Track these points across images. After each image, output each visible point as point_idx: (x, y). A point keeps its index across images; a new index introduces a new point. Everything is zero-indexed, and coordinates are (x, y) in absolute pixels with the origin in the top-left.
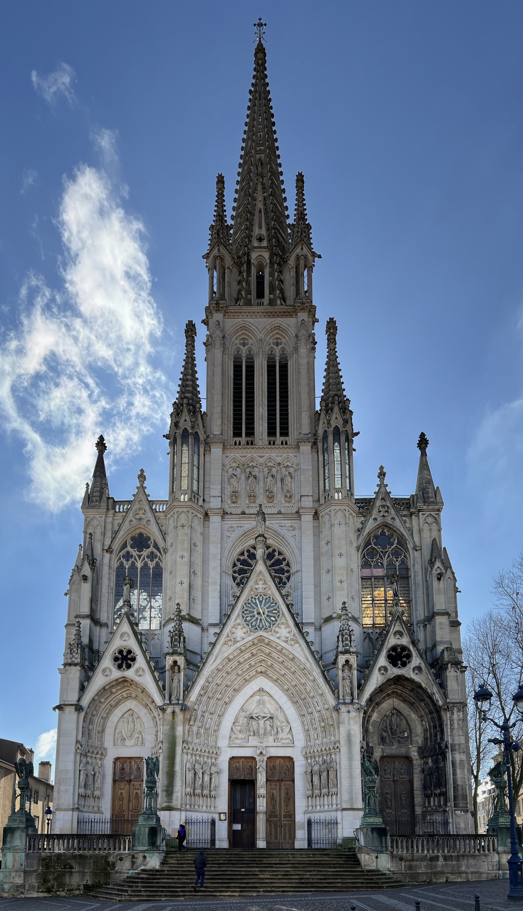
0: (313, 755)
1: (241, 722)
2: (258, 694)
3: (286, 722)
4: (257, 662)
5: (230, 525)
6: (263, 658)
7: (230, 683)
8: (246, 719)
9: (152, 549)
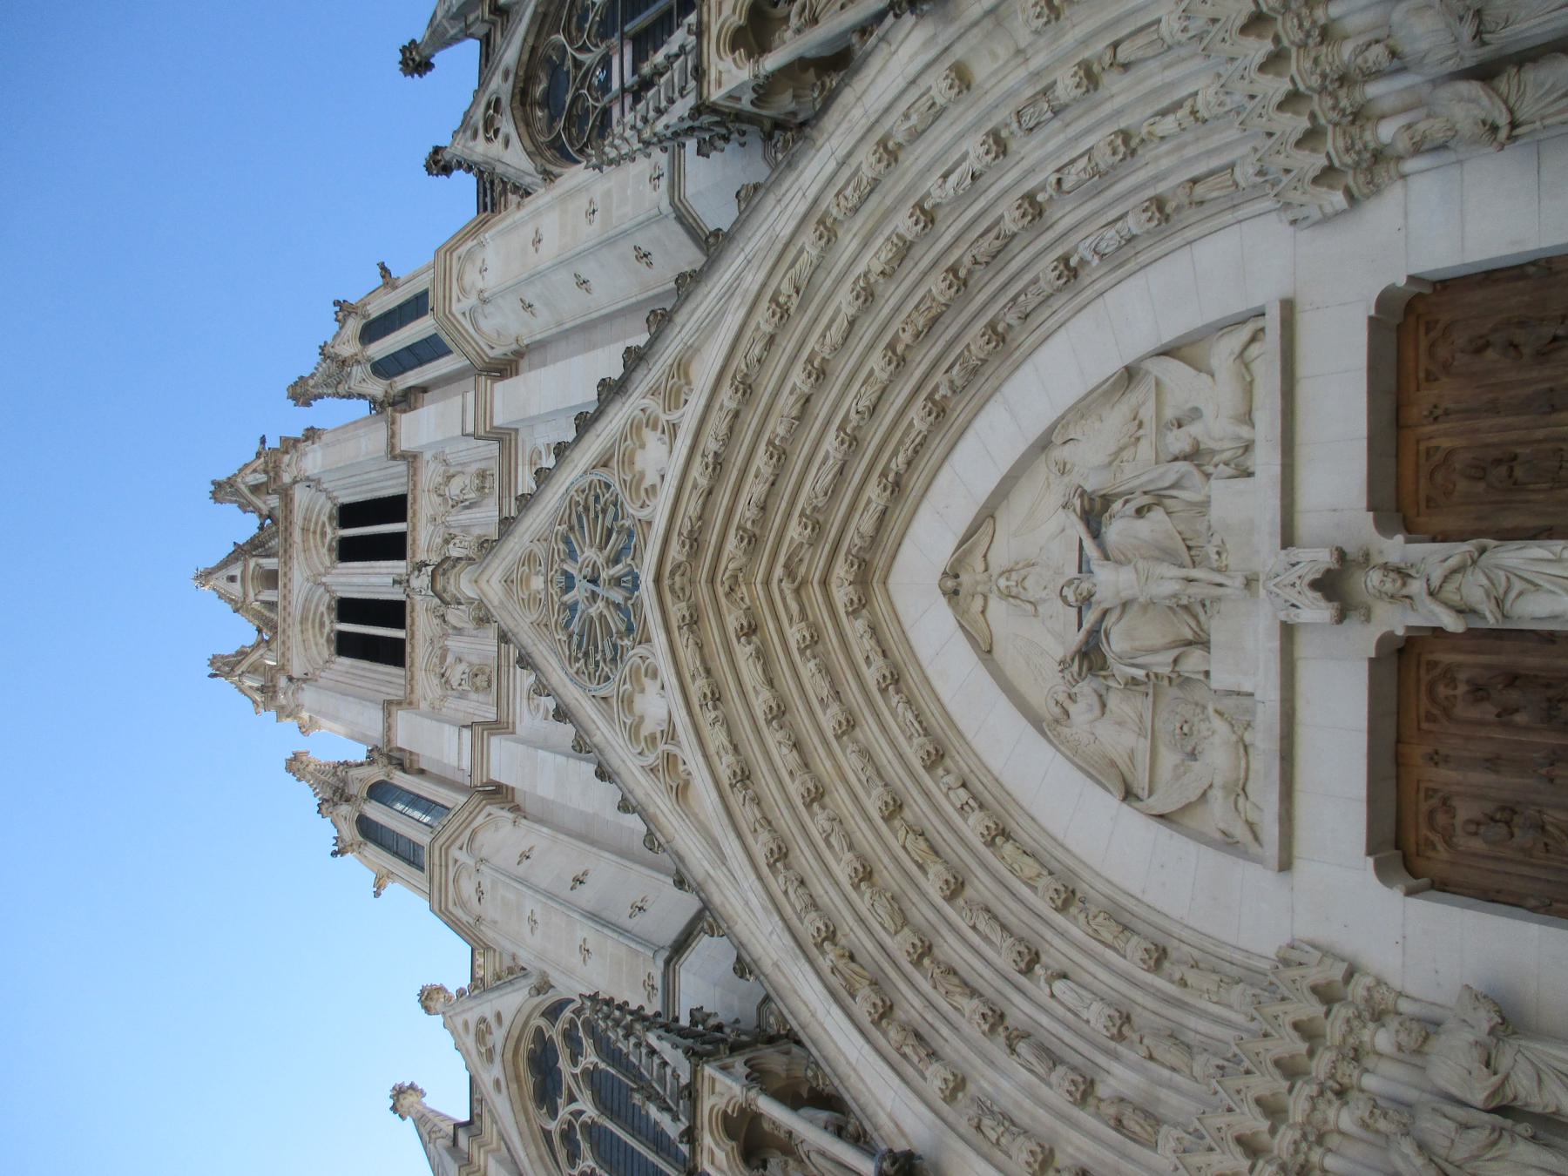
0: (1321, 106)
2: (978, 604)
3: (1133, 398)
4: (794, 607)
5: (525, 701)
6: (779, 571)
8: (1113, 701)
9: (555, 1033)
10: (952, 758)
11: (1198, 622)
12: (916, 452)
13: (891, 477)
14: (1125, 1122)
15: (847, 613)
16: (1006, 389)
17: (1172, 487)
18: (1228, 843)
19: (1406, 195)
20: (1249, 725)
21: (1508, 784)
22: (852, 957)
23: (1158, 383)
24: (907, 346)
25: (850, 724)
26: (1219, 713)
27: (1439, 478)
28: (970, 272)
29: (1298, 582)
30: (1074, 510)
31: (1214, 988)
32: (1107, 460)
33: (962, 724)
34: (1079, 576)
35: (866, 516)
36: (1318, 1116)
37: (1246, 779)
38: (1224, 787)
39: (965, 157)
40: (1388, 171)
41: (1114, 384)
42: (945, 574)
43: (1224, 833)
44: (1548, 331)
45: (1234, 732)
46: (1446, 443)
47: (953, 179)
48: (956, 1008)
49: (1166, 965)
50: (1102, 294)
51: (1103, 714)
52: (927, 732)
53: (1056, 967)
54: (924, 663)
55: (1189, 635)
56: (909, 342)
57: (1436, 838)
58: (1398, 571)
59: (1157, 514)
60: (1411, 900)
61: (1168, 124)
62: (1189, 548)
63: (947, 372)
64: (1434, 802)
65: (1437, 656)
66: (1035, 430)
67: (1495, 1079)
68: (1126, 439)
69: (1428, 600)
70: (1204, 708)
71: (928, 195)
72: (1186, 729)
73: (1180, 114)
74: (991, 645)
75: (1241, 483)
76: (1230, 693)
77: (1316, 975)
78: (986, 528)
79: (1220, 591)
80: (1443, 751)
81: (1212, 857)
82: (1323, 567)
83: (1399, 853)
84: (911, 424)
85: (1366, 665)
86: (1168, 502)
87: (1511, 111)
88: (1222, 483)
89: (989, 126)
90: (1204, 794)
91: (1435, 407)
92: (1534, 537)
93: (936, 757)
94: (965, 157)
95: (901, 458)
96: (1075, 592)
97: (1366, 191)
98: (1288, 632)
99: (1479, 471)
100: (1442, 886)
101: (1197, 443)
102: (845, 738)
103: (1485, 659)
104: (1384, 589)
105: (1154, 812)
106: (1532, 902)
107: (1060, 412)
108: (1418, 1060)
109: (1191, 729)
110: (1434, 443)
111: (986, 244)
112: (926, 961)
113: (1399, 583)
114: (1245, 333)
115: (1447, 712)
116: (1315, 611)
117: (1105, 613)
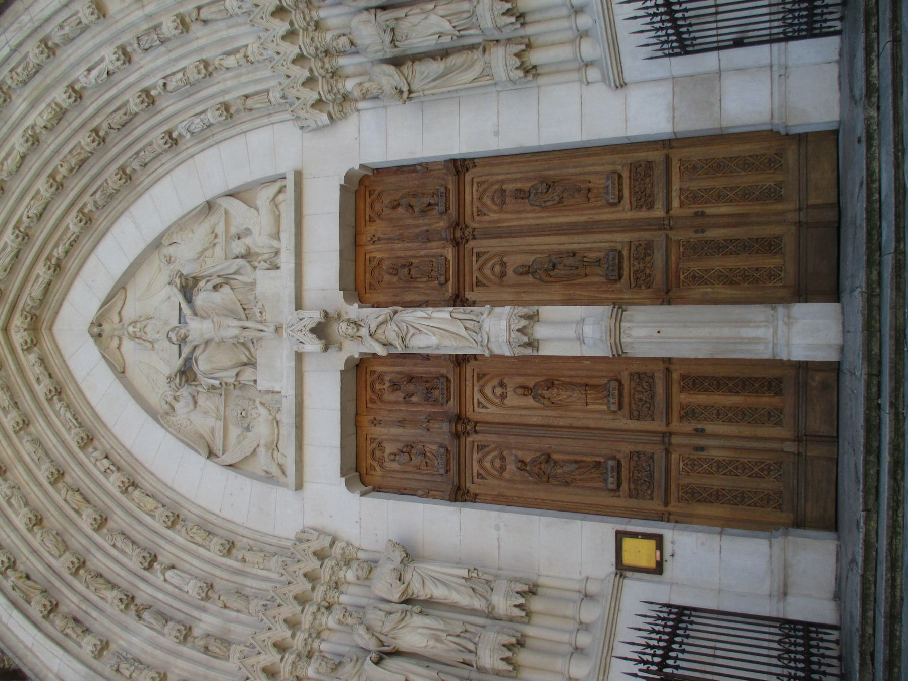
0: (316, 64)
1: (211, 422)
7: (46, 465)
8: (201, 400)
10: (99, 440)
11: (250, 352)
12: (71, 245)
13: (54, 261)
14: (210, 648)
15: (23, 350)
16: (135, 209)
17: (234, 273)
18: (268, 478)
19: (359, 121)
20: (279, 410)
21: (408, 433)
22: (28, 577)
23: (226, 212)
24: (64, 177)
25: (25, 423)
26: (262, 403)
27: (376, 273)
28: (107, 133)
29: (304, 329)
30: (176, 286)
31: (261, 561)
32: (196, 256)
33: (105, 419)
34: (178, 325)
35: (36, 286)
36: (317, 622)
37: (278, 440)
38: (266, 446)
39: (102, 60)
40: (350, 106)
41: (200, 211)
42: (92, 324)
43: (266, 472)
44: (426, 200)
45: (271, 414)
46: (379, 255)
47: (94, 73)
48: (102, 598)
49: (234, 551)
50: (192, 156)
51: (195, 407)
52: (81, 425)
53: (167, 562)
54: (79, 380)
55: (245, 360)
56: (66, 174)
57: (375, 464)
58: (355, 323)
59: (226, 289)
60: (364, 499)
61: (231, 61)
62: (244, 309)
63: (92, 195)
64: (374, 445)
65: (376, 368)
66: (151, 237)
67: (404, 586)
68: (208, 245)
69: (369, 338)
70: (254, 401)
71: (77, 80)
72: (244, 414)
73: (238, 56)
74: (124, 368)
75: (273, 273)
76: (268, 392)
77: (315, 545)
78: (121, 295)
79: (262, 334)
80: (378, 418)
81: (258, 486)
82: (317, 321)
83: (358, 473)
84: (67, 228)
85: (338, 376)
86: (232, 282)
87: (409, 85)
88: (262, 272)
89: (119, 43)
90: (255, 450)
91: (374, 236)
92: (420, 306)
93: (88, 441)
94: (102, 60)
95: (61, 250)
96: (176, 335)
97: (339, 116)
98: (299, 357)
99: (394, 271)
100: (378, 489)
101: (249, 248)
102: (22, 433)
103: (397, 369)
104: (348, 333)
105: (226, 464)
106: (420, 492)
107: (167, 226)
108: (367, 583)
109: (246, 414)
110: (374, 255)
111: (118, 118)
112: (82, 572)
113: (355, 330)
114: (276, 187)
115: (380, 397)
116: (313, 345)
117: (195, 348)
